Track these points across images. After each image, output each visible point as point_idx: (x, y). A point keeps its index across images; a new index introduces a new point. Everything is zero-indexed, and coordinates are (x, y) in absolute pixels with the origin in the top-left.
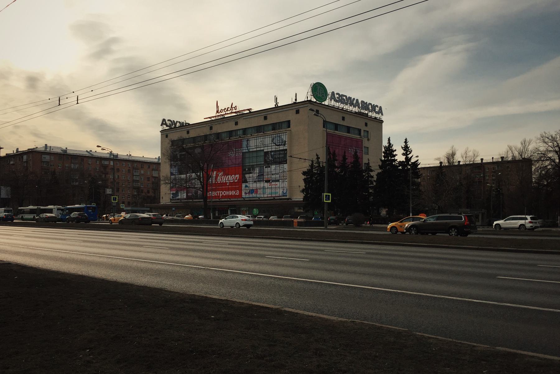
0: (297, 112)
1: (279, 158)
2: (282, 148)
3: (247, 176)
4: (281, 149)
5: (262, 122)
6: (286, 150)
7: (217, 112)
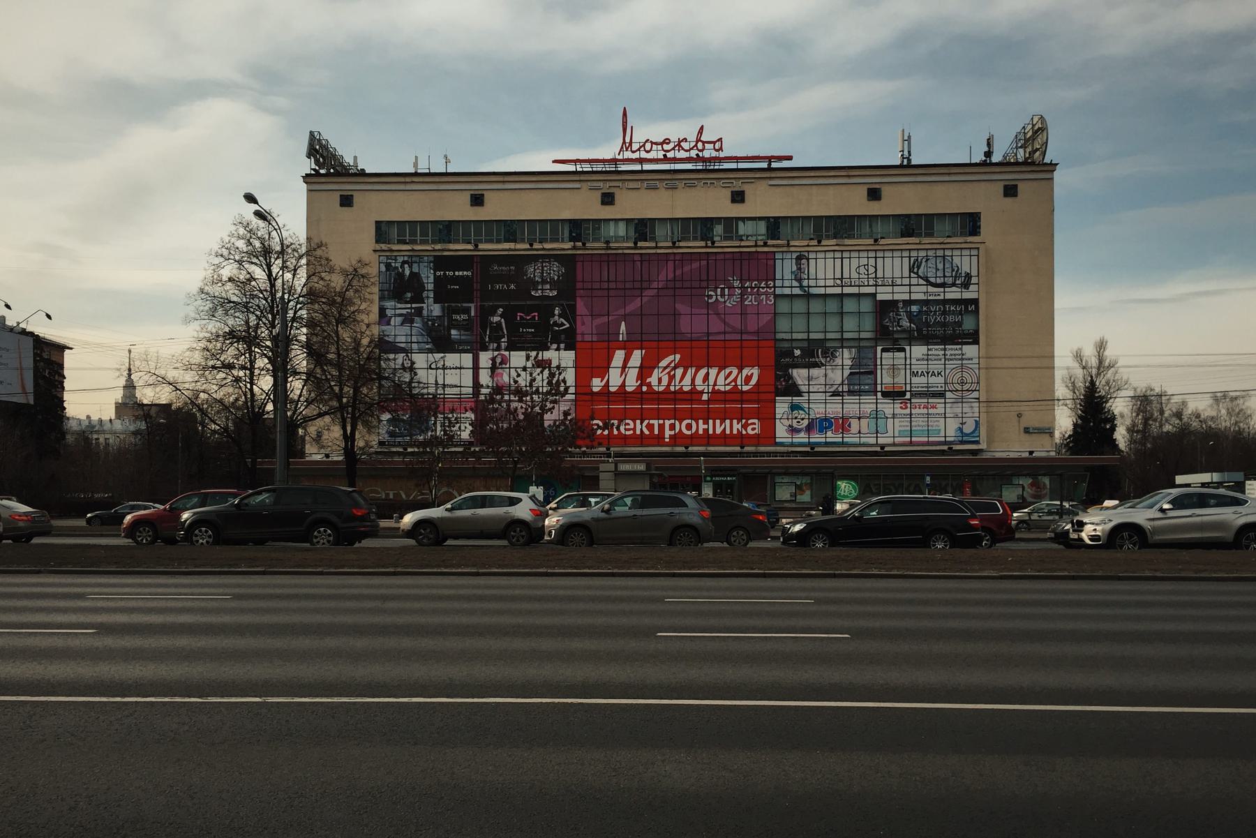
0: (1010, 191)
1: (944, 325)
2: (953, 294)
3: (799, 375)
4: (949, 296)
5: (853, 203)
6: (975, 302)
7: (626, 146)
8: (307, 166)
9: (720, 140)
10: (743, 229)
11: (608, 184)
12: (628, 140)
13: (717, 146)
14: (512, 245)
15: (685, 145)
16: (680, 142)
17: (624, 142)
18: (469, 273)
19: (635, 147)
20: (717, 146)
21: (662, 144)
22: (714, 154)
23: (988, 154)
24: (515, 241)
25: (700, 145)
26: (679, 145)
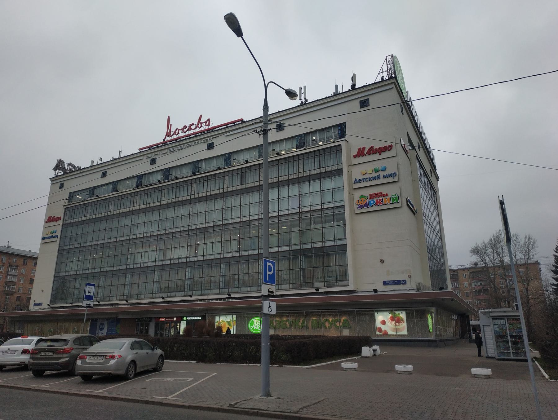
0: (364, 104)
7: (168, 134)
9: (209, 120)
11: (154, 154)
15: (193, 127)
19: (172, 133)
21: (183, 129)
22: (207, 127)
25: (200, 125)
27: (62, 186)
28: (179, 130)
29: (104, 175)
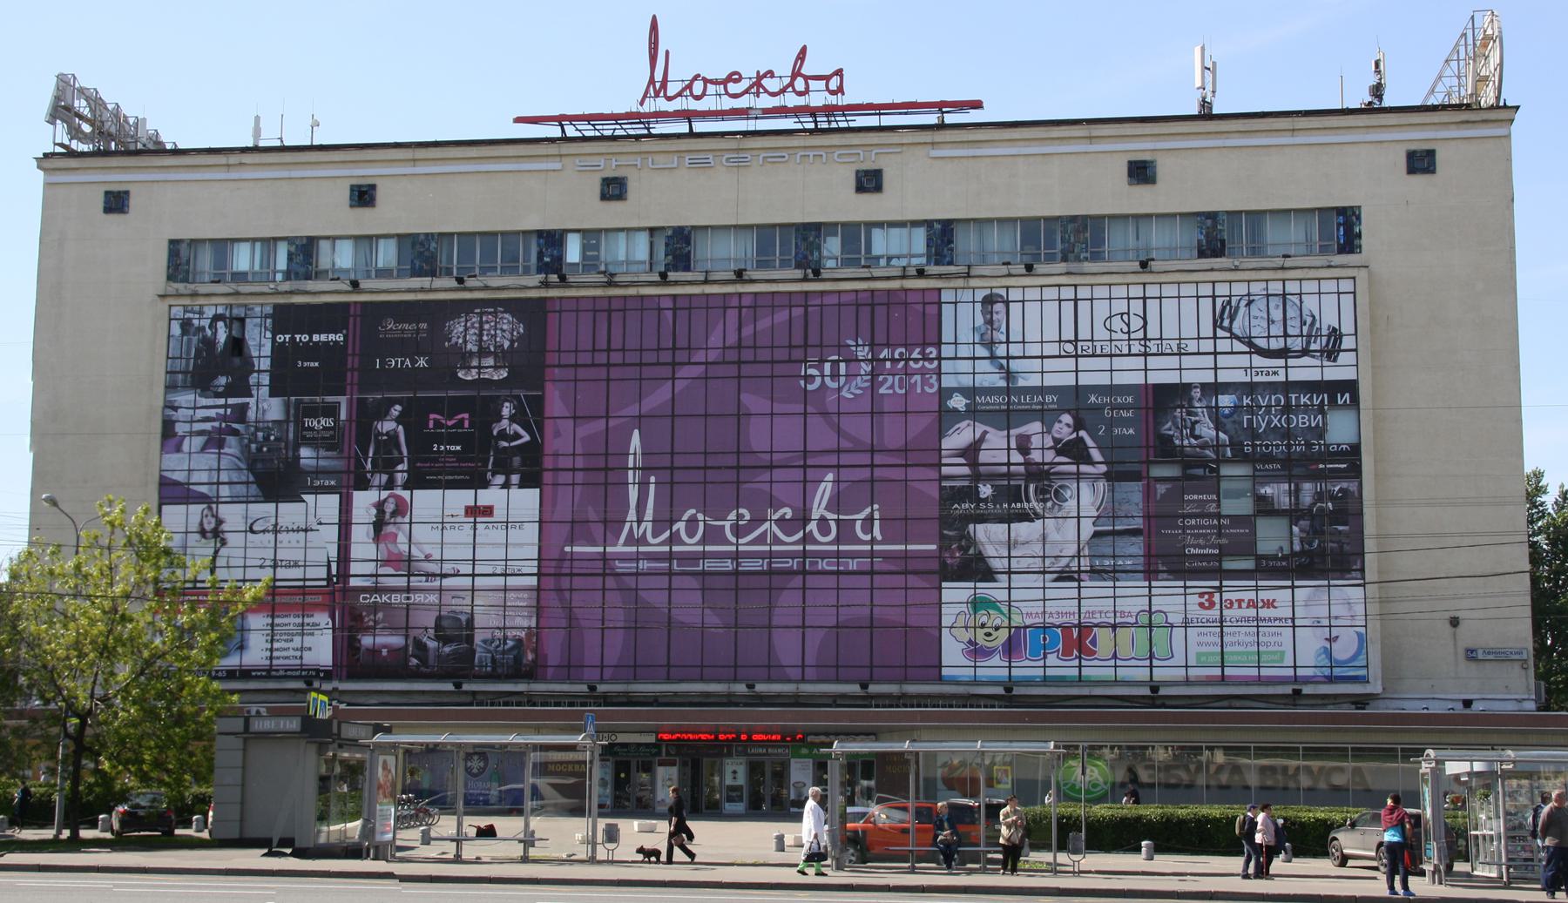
1: (1287, 434)
2: (1305, 370)
3: (989, 537)
4: (1296, 375)
5: (1099, 188)
6: (1351, 387)
7: (657, 87)
8: (50, 137)
9: (839, 73)
10: (881, 243)
12: (659, 76)
13: (834, 84)
14: (425, 282)
16: (760, 77)
17: (652, 81)
18: (340, 337)
20: (834, 84)
21: (725, 82)
23: (1377, 91)
24: (433, 274)
25: (800, 84)
26: (757, 85)
27: (116, 203)
28: (706, 81)
29: (363, 196)
